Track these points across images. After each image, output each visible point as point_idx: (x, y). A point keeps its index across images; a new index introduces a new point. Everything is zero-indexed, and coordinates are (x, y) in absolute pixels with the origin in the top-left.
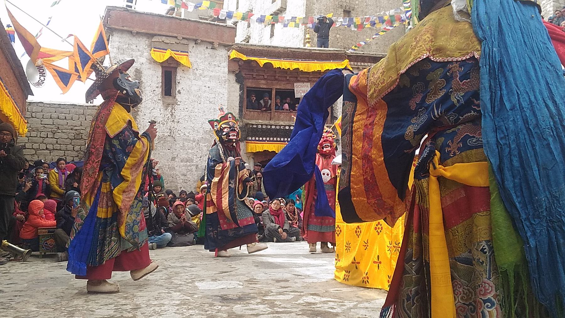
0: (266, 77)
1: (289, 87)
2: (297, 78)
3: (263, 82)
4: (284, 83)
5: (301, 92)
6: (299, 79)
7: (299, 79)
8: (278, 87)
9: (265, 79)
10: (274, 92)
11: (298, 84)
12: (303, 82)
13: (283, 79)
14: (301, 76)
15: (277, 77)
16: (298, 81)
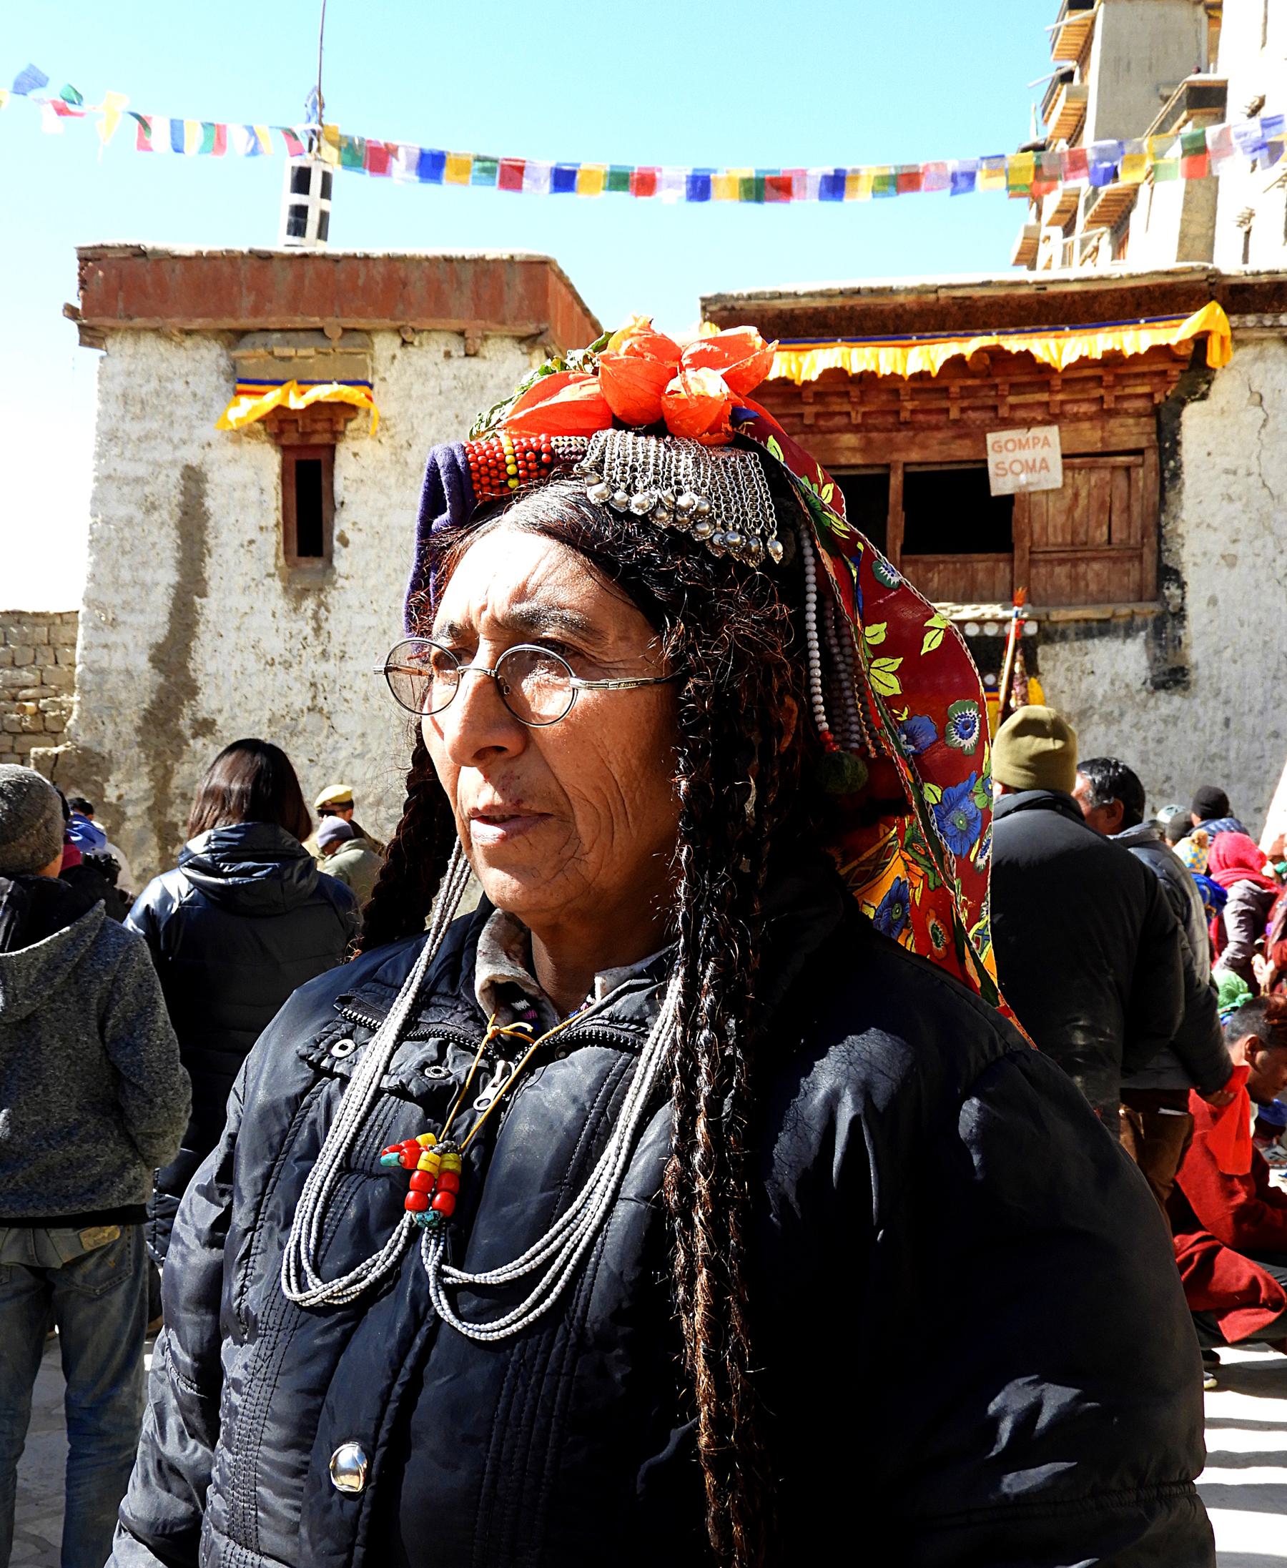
0: (857, 419)
1: (962, 450)
2: (995, 408)
3: (849, 439)
4: (940, 435)
5: (1017, 467)
6: (1004, 412)
7: (1004, 412)
8: (915, 456)
9: (855, 429)
10: (896, 481)
11: (1005, 435)
12: (1028, 424)
13: (933, 419)
14: (1012, 400)
15: (905, 415)
16: (1007, 424)
